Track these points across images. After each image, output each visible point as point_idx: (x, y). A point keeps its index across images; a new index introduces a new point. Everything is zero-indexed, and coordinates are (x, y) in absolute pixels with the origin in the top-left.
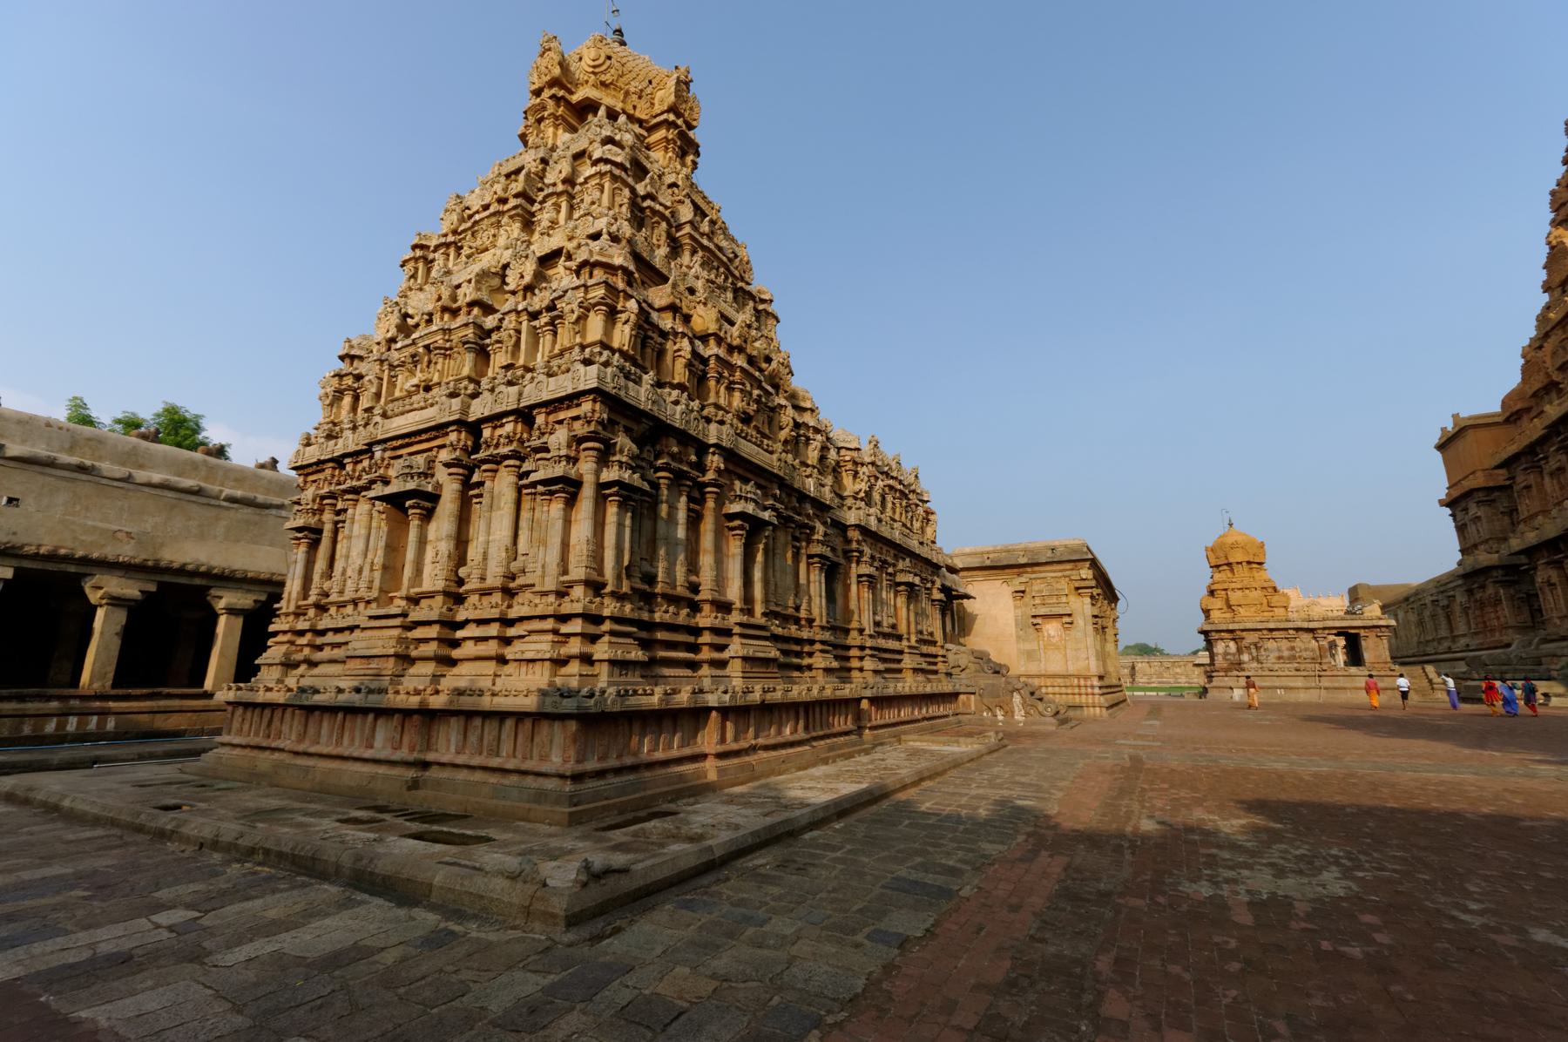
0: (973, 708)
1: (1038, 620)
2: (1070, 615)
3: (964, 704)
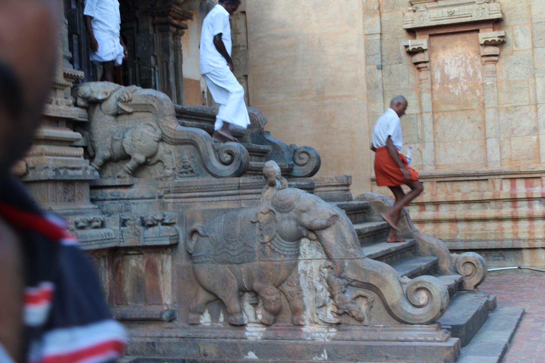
0: (168, 299)
1: (422, 42)
2: (496, 23)
3: (139, 285)
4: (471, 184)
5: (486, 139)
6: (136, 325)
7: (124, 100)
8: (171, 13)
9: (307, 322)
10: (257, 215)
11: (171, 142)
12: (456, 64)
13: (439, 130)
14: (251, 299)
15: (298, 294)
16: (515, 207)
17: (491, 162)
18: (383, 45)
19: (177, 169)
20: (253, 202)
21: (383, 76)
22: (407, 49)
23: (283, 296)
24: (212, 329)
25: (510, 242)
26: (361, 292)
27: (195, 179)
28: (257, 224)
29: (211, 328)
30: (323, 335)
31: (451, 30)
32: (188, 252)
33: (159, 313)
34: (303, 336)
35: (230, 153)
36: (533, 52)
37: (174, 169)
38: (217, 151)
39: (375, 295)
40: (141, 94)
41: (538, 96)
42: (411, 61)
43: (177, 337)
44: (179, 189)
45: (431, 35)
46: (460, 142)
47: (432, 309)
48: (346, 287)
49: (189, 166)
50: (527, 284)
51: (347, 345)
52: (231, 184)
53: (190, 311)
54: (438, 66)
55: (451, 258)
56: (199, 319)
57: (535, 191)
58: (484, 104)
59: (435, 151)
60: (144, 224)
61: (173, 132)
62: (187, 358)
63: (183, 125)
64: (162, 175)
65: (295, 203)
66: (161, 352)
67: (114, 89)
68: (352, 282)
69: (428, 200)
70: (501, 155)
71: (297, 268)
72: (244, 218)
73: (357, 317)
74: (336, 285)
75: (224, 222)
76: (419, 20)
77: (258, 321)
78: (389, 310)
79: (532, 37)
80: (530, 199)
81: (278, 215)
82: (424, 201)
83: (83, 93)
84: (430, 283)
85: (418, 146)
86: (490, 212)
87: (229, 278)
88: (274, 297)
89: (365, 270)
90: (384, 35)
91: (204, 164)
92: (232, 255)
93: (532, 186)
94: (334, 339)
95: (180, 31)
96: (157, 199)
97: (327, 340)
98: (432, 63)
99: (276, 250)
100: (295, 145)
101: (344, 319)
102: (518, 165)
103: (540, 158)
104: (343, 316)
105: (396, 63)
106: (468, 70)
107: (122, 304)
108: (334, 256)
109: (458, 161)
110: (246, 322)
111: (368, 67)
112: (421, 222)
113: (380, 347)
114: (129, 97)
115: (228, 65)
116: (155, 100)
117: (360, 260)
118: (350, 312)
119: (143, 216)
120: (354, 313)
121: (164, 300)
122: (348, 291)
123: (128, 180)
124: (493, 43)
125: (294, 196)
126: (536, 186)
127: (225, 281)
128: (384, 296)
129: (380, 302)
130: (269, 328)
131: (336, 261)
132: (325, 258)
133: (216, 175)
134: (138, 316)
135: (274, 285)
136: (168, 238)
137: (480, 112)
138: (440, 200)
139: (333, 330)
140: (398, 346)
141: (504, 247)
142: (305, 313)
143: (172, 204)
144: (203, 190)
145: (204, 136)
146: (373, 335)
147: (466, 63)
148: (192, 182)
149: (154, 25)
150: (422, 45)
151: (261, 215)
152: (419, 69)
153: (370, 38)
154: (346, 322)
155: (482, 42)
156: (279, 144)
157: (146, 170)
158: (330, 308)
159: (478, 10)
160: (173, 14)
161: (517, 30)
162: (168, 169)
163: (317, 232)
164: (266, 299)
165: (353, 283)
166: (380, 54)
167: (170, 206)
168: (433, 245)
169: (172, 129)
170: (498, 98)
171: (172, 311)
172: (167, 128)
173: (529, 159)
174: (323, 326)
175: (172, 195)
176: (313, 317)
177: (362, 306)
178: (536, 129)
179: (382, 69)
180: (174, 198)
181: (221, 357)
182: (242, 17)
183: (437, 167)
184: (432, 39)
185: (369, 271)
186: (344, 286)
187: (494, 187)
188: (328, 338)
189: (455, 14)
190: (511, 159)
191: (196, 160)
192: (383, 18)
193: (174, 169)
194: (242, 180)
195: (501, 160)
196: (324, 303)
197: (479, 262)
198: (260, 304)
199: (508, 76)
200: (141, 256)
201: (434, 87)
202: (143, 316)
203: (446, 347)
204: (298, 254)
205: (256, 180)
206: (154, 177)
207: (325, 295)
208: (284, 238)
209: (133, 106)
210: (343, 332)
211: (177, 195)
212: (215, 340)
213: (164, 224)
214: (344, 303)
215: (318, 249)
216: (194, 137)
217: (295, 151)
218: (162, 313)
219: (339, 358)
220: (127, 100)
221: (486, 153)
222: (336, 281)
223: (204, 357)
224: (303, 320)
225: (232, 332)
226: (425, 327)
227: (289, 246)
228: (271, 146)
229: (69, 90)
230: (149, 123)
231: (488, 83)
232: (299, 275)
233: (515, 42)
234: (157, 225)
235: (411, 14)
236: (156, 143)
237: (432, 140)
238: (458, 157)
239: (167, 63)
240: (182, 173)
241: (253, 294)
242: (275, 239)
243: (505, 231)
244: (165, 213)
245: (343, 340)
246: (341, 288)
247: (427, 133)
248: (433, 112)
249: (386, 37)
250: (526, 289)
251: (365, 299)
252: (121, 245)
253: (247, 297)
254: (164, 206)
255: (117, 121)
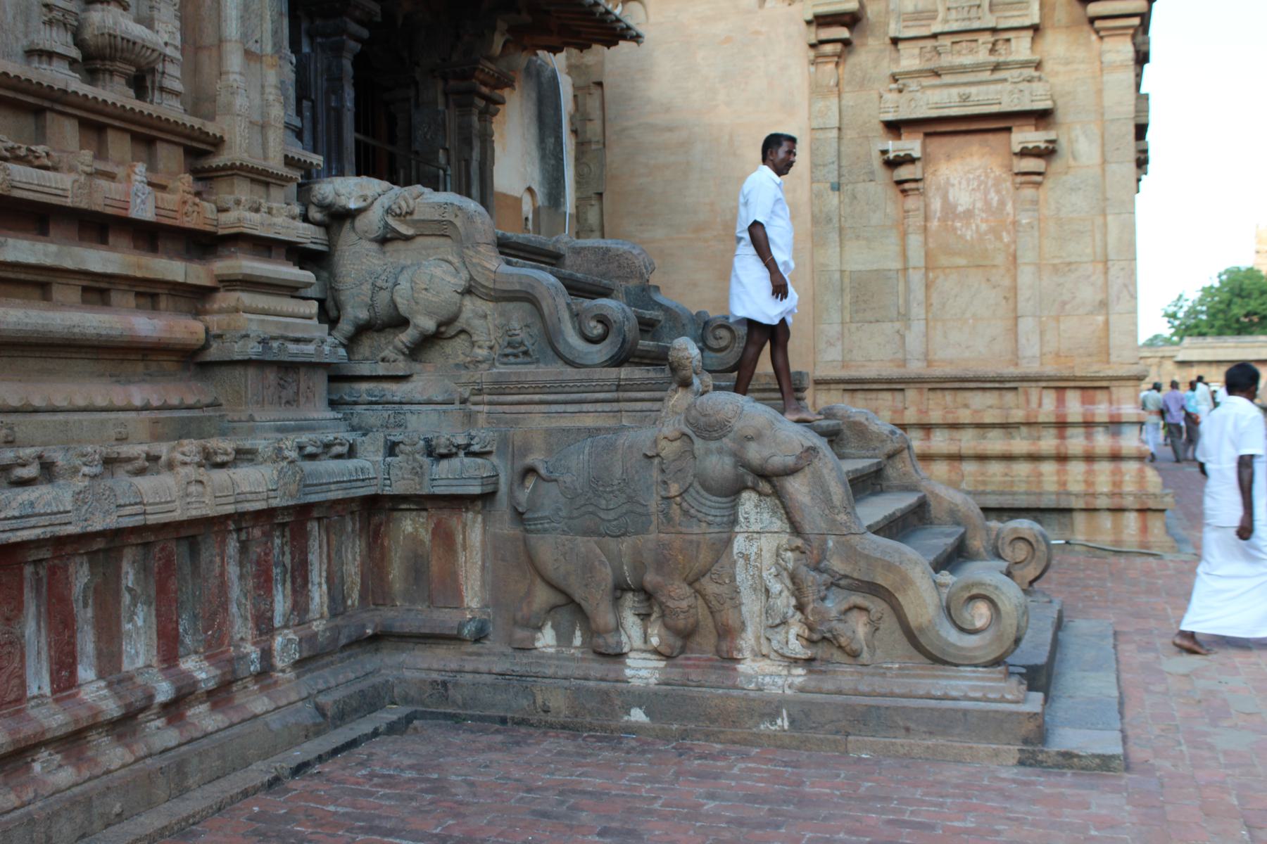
0: (473, 598)
1: (911, 144)
2: (1042, 117)
3: (417, 569)
4: (988, 394)
5: (1016, 318)
6: (411, 646)
7: (398, 211)
8: (477, 73)
9: (747, 654)
10: (655, 442)
11: (487, 295)
12: (968, 185)
13: (935, 299)
14: (636, 605)
15: (732, 599)
16: (1062, 437)
17: (1024, 358)
18: (843, 149)
19: (497, 346)
20: (646, 417)
21: (840, 202)
22: (886, 157)
23: (700, 601)
24: (558, 659)
25: (1054, 497)
26: (857, 599)
27: (532, 368)
28: (656, 461)
29: (557, 656)
30: (780, 681)
31: (964, 127)
32: (516, 510)
33: (456, 625)
34: (740, 681)
35: (602, 320)
36: (1104, 170)
37: (491, 348)
38: (577, 315)
39: (884, 605)
40: (431, 201)
41: (1110, 247)
42: (892, 178)
43: (490, 673)
44: (500, 387)
45: (927, 135)
46: (971, 321)
47: (999, 638)
48: (827, 589)
49: (522, 343)
50: (1089, 572)
51: (830, 704)
52: (603, 380)
53: (515, 623)
54: (938, 189)
55: (988, 530)
56: (534, 639)
57: (1097, 411)
58: (1015, 257)
59: (926, 335)
60: (434, 453)
61: (492, 275)
62: (509, 715)
63: (509, 263)
64: (469, 359)
65: (733, 421)
66: (460, 702)
67: (380, 191)
68: (840, 579)
69: (913, 421)
70: (1042, 346)
71: (732, 548)
72: (630, 447)
73: (848, 649)
74: (810, 584)
75: (590, 454)
76: (909, 106)
77: (651, 648)
78: (911, 636)
79: (1103, 145)
80: (1089, 425)
81: (699, 444)
82: (906, 422)
83: (320, 197)
84: (996, 588)
85: (897, 325)
86: (1020, 445)
87: (597, 563)
88: (684, 604)
89: (867, 557)
90: (844, 131)
92: (603, 520)
93: (1092, 402)
94: (802, 690)
95: (492, 107)
96: (457, 406)
97: (788, 692)
98: (928, 182)
99: (692, 511)
100: (705, 313)
101: (821, 651)
102: (1071, 364)
103: (1108, 354)
104: (820, 645)
105: (864, 181)
106: (989, 197)
107: (384, 605)
108: (807, 528)
109: (967, 354)
110: (625, 650)
111: (815, 185)
112: (926, 458)
113: (896, 709)
114: (408, 206)
116: (459, 213)
117: (857, 538)
118: (835, 637)
119: (429, 436)
120: (843, 641)
121: (466, 600)
122: (831, 596)
123: (401, 367)
124: (1034, 152)
125: (731, 407)
126: (1100, 403)
127: (588, 568)
128: (902, 609)
129: (894, 619)
130: (671, 662)
131: (811, 537)
132: (788, 530)
133: (574, 362)
134: (415, 630)
135: (685, 580)
136: (478, 482)
137: (1008, 270)
138: (933, 422)
139: (800, 671)
140: (932, 709)
141: (1042, 506)
142: (744, 635)
143: (485, 416)
144: (548, 390)
145: (553, 285)
146: (879, 684)
147: (986, 184)
148: (526, 374)
149: (446, 94)
150: (912, 149)
151: (664, 443)
152: (904, 191)
153: (819, 135)
154: (825, 656)
155: (1017, 149)
156: (677, 310)
157: (437, 347)
158: (795, 629)
159: (1011, 92)
160: (481, 77)
161: (1077, 131)
162: (480, 347)
163: (775, 479)
164: (668, 607)
165: (842, 582)
166: (836, 163)
167: (481, 419)
168: (956, 505)
169: (491, 271)
170: (1040, 247)
171: (479, 621)
172: (479, 269)
173: (1090, 355)
174: (778, 663)
175: (486, 398)
176: (759, 644)
177: (859, 628)
178: (1104, 305)
179: (839, 189)
180: (490, 403)
181: (576, 716)
182: (596, 92)
183: (929, 363)
184: (929, 141)
185: (877, 559)
186: (824, 588)
187: (1028, 401)
188: (789, 687)
189: (971, 99)
190: (1058, 355)
191: (535, 330)
192: (844, 102)
193: (491, 348)
194: (625, 372)
195: (1042, 355)
196: (784, 618)
197: (1040, 538)
198: (654, 616)
199: (1059, 210)
200: (424, 514)
201: (929, 225)
202: (426, 630)
203: (1028, 713)
204: (734, 522)
205: (652, 375)
206: (451, 361)
207: (784, 601)
208: (708, 489)
209: (415, 223)
210: (820, 677)
211: (495, 398)
212: (566, 683)
213: (469, 454)
214: (823, 620)
215: (774, 513)
216: (533, 287)
217: (706, 323)
218: (461, 626)
219: (811, 728)
220: (404, 213)
221: (1016, 341)
222: (810, 577)
223: (542, 713)
224: (740, 651)
225: (598, 668)
226: (982, 672)
227: (717, 505)
228: (663, 313)
229: (293, 188)
230: (446, 257)
231: (1024, 221)
232: (735, 562)
233: (1073, 153)
234: (456, 454)
235: (895, 95)
236: (458, 296)
237: (923, 316)
238: (968, 347)
239: (468, 163)
240: (506, 355)
241: (642, 597)
242: (691, 490)
243: (1044, 479)
244: (473, 433)
245: (821, 692)
246: (819, 591)
247: (915, 305)
248: (927, 268)
249: (849, 134)
250: (1092, 583)
251: (864, 613)
252: (385, 493)
253: (630, 599)
254: (470, 418)
255: (384, 253)
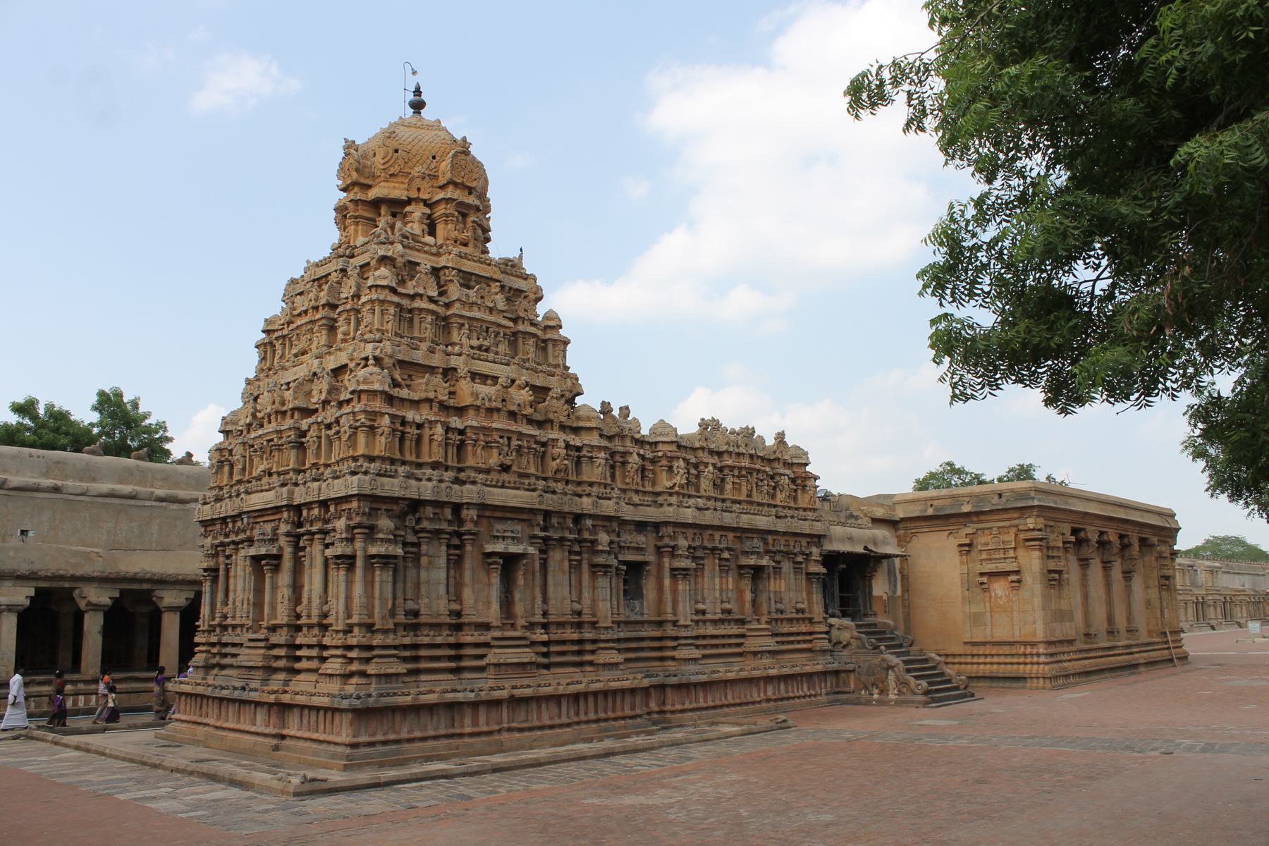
0: (852, 686)
1: (985, 579)
2: (1017, 572)
3: (844, 682)
44: (856, 653)
91: (864, 645)
115: (1024, 472)
249: (971, 575)
